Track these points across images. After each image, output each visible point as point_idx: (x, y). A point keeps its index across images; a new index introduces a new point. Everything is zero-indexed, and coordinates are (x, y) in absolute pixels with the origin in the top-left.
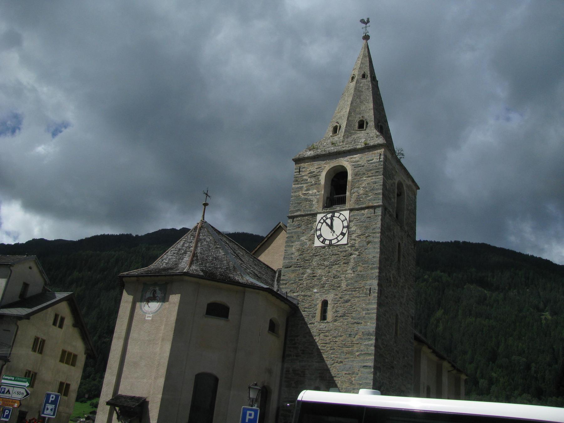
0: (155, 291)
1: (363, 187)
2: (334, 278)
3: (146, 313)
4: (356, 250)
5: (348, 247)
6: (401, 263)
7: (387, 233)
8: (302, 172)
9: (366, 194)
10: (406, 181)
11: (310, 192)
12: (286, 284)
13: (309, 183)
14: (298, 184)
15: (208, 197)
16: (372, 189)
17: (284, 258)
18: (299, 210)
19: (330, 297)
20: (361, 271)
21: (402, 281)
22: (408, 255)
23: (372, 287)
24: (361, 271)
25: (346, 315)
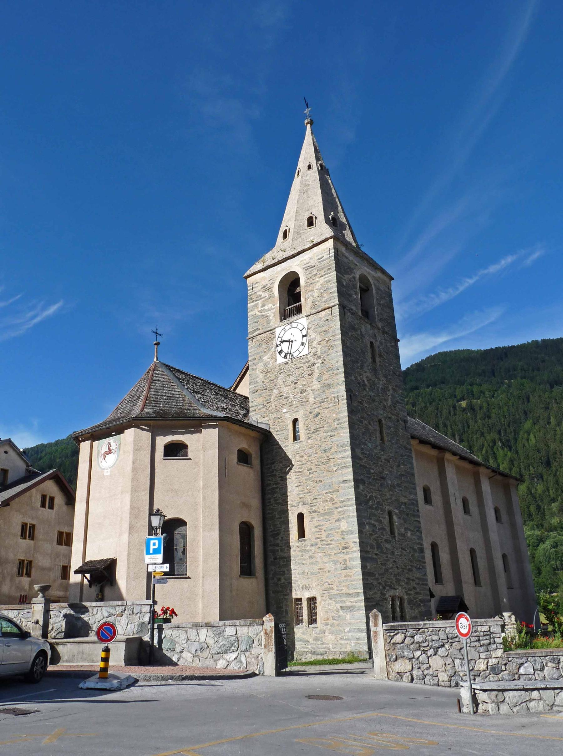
0: (110, 444)
1: (317, 289)
2: (301, 393)
3: (104, 469)
4: (319, 357)
5: (310, 356)
6: (378, 364)
7: (350, 334)
8: (255, 288)
9: (321, 296)
10: (373, 273)
11: (266, 307)
12: (255, 410)
13: (263, 298)
14: (253, 302)
15: (158, 336)
16: (327, 289)
17: (250, 384)
18: (257, 329)
19: (300, 416)
20: (326, 380)
21: (381, 383)
22: (387, 353)
23: (340, 394)
24: (326, 380)
25: (318, 430)
